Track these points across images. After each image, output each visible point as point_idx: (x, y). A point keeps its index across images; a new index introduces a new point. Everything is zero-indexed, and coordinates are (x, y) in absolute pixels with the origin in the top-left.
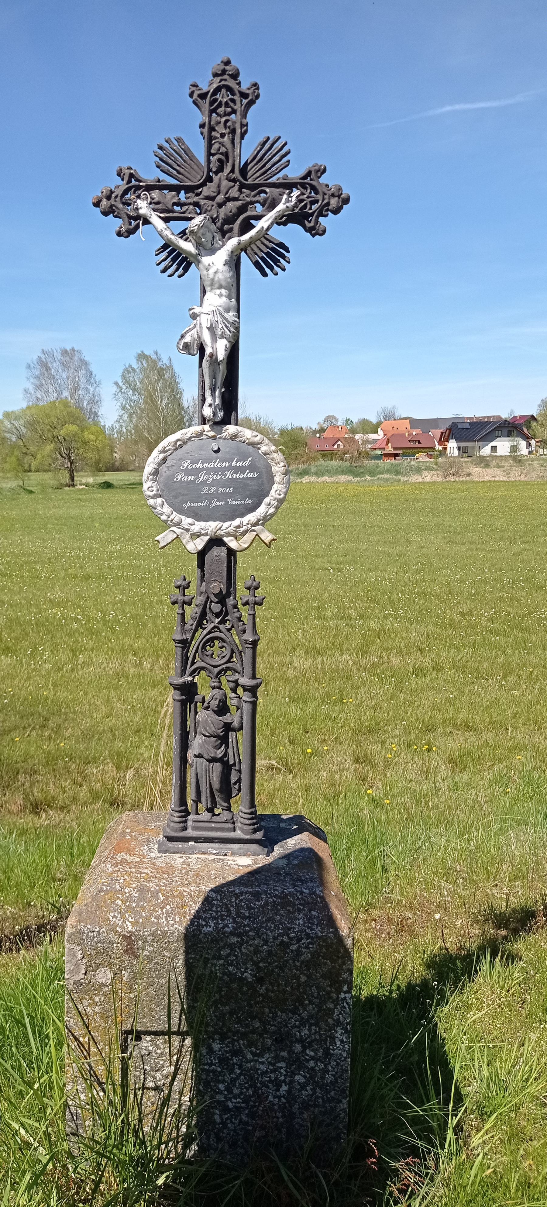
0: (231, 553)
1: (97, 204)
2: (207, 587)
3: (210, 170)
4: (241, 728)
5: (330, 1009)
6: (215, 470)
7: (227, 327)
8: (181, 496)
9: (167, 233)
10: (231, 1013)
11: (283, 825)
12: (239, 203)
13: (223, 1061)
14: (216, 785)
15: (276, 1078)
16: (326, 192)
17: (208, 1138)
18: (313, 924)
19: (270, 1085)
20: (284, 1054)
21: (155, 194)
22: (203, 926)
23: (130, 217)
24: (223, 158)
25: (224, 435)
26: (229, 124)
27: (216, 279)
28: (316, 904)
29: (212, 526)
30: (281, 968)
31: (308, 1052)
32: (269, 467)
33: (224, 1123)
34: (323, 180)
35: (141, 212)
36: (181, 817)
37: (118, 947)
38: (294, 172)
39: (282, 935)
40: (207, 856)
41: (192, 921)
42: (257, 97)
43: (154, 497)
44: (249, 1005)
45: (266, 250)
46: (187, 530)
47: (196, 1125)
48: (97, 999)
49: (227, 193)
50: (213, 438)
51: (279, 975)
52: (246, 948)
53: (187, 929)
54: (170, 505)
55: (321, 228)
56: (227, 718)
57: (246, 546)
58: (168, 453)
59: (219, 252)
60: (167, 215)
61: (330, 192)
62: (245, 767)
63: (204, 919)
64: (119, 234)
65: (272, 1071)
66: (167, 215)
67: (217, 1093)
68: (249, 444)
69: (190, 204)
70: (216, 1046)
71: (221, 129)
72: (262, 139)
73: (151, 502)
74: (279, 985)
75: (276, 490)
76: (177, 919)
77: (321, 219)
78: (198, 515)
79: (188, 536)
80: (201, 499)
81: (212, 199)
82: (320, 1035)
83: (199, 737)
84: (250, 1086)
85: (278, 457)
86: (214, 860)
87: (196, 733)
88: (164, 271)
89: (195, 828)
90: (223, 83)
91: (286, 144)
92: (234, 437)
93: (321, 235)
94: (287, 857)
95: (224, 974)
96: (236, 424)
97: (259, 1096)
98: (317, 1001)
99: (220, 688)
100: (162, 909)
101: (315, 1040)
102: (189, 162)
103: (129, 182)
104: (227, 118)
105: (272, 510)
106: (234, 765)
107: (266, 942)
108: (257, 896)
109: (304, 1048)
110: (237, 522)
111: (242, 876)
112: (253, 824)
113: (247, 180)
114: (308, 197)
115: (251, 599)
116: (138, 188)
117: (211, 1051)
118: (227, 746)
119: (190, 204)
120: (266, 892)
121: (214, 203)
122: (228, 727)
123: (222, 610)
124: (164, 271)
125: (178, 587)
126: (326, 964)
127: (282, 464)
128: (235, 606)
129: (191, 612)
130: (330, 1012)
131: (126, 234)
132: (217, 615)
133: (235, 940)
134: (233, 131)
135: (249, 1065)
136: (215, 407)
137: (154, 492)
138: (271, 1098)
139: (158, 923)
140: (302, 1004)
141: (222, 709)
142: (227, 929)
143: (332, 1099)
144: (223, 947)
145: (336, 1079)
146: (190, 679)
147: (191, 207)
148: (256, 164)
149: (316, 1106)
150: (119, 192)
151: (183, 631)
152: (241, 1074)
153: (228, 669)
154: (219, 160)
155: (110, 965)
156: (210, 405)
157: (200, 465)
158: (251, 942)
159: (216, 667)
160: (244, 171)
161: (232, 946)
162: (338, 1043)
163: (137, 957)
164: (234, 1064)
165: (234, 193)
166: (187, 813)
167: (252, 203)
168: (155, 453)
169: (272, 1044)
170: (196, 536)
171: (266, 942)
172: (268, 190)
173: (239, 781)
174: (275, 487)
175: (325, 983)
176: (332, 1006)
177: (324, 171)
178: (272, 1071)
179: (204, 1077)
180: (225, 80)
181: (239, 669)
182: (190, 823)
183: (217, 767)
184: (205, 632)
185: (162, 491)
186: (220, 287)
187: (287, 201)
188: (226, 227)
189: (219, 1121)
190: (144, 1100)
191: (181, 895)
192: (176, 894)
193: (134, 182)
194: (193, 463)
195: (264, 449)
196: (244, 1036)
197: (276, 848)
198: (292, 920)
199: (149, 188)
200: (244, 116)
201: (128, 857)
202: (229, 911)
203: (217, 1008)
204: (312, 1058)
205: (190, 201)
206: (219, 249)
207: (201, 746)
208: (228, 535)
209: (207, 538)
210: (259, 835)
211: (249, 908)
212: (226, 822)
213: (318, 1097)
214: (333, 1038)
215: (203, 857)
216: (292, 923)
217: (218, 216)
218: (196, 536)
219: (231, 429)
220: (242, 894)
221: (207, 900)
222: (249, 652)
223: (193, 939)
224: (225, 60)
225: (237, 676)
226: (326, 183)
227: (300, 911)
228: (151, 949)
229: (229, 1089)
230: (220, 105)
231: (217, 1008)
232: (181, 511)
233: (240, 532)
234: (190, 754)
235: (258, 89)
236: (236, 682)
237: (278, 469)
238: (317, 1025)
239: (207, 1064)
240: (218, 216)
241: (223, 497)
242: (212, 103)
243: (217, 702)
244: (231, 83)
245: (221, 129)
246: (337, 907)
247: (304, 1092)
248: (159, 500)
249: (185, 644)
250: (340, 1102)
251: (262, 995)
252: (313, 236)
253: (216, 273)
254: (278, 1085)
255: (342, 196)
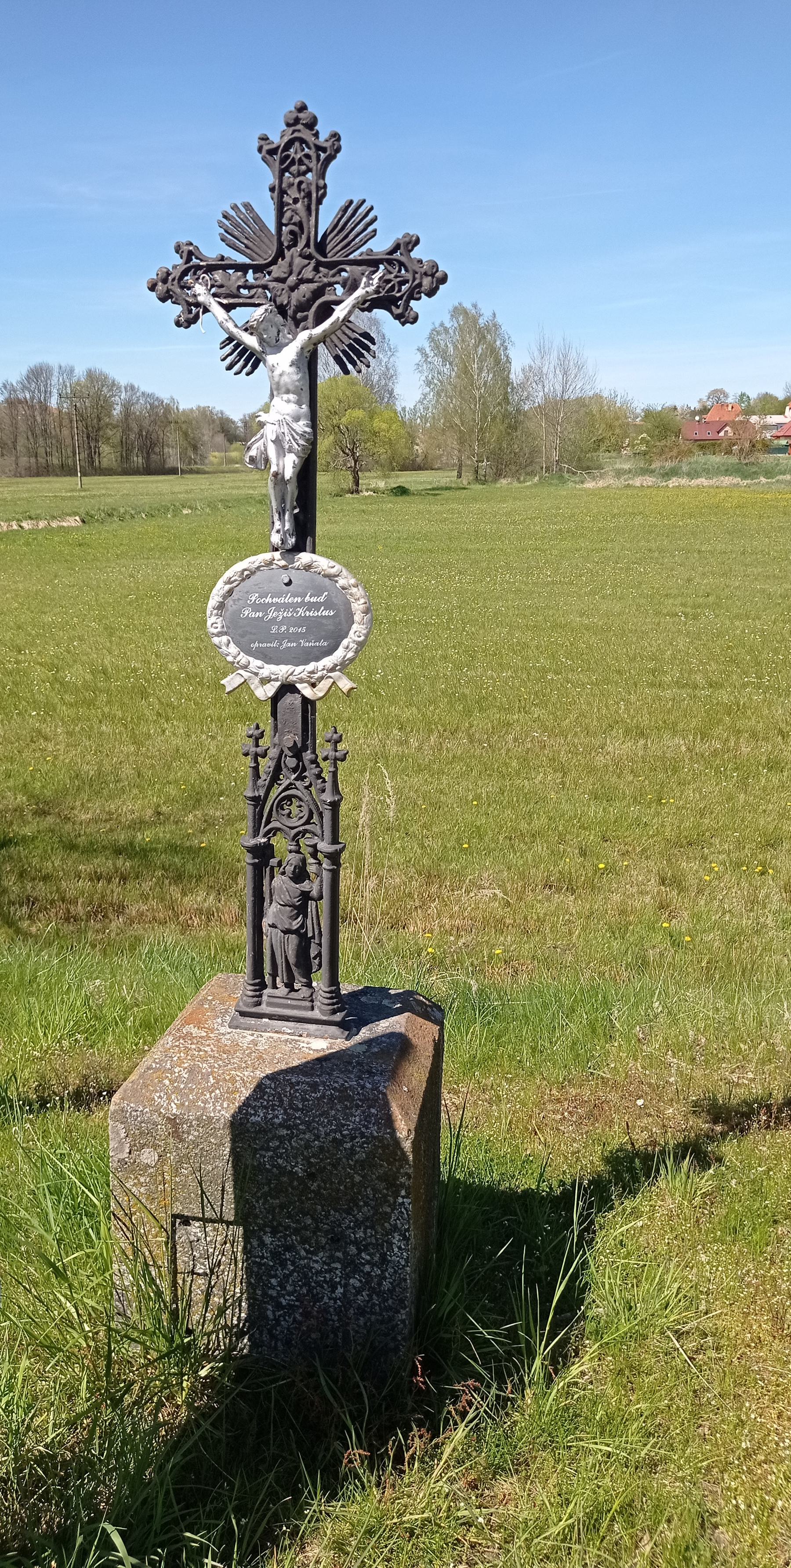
0: (306, 702)
1: (152, 288)
2: (280, 740)
3: (280, 243)
4: (321, 897)
5: (386, 1213)
6: (286, 606)
7: (295, 440)
8: (251, 635)
9: (230, 325)
10: (282, 1207)
11: (386, 1002)
12: (314, 286)
13: (275, 1255)
14: (292, 960)
15: (331, 1279)
16: (418, 270)
17: (261, 1334)
18: (369, 1122)
19: (325, 1286)
20: (339, 1254)
21: (218, 275)
22: (251, 1115)
23: (189, 304)
24: (296, 229)
25: (297, 564)
26: (303, 186)
27: (282, 382)
28: (376, 1101)
29: (282, 671)
30: (334, 1166)
31: (363, 1255)
32: (348, 604)
33: (277, 1321)
34: (416, 254)
35: (201, 299)
36: (255, 991)
37: (162, 1129)
38: (380, 245)
39: (335, 1131)
40: (280, 1036)
41: (240, 1107)
42: (338, 150)
43: (219, 634)
44: (300, 1200)
45: (347, 341)
46: (256, 674)
47: (246, 1320)
48: (142, 1180)
49: (299, 273)
50: (285, 568)
51: (331, 1173)
52: (296, 1142)
53: (233, 1116)
54: (237, 644)
55: (412, 314)
56: (305, 886)
57: (321, 694)
58: (234, 584)
59: (285, 349)
60: (232, 301)
61: (423, 270)
62: (325, 940)
63: (254, 1108)
64: (178, 324)
65: (326, 1271)
66: (232, 301)
67: (270, 1288)
68: (325, 576)
69: (258, 287)
70: (268, 1239)
71: (294, 193)
72: (342, 203)
73: (216, 640)
74: (332, 1183)
75: (357, 631)
76: (225, 1105)
77: (413, 303)
78: (268, 657)
79: (256, 681)
80: (270, 638)
81: (283, 280)
82: (377, 1239)
83: (274, 904)
84: (304, 1285)
85: (358, 592)
86: (287, 1041)
87: (271, 901)
88: (229, 368)
89: (269, 1004)
90: (296, 135)
91: (372, 208)
92: (308, 567)
93: (412, 323)
94: (369, 1042)
95: (273, 1166)
96: (314, 552)
97: (313, 1296)
98: (373, 1203)
99: (298, 852)
100: (211, 1093)
101: (371, 1243)
102: (259, 233)
103: (189, 260)
104: (301, 178)
105: (350, 655)
106: (313, 937)
107: (317, 1137)
108: (314, 1087)
109: (360, 1251)
110: (311, 666)
111: (308, 1062)
112: (333, 1004)
113: (326, 257)
114: (396, 277)
115: (332, 754)
116: (198, 267)
117: (262, 1244)
118: (305, 916)
119: (258, 287)
120: (324, 1084)
121: (285, 286)
122: (306, 896)
123: (298, 765)
124: (229, 368)
125: (250, 736)
126: (382, 1166)
127: (362, 601)
128: (314, 761)
129: (266, 765)
130: (386, 1217)
131: (185, 324)
132: (294, 770)
133: (285, 1132)
134: (309, 195)
135: (302, 1262)
136: (285, 533)
137: (219, 630)
138: (326, 1299)
139: (205, 1108)
140: (357, 1205)
141: (300, 875)
142: (276, 1120)
143: (390, 1308)
144: (272, 1139)
145: (394, 1288)
146: (264, 840)
147: (260, 290)
148: (337, 235)
149: (372, 1313)
150: (176, 274)
151: (255, 787)
152: (293, 1271)
153: (306, 831)
154: (292, 232)
155: (155, 1147)
156: (278, 531)
157: (268, 600)
158: (301, 1136)
159: (292, 828)
160: (321, 247)
161: (281, 1139)
162: (396, 1250)
163: (182, 1140)
164: (286, 1259)
165: (308, 273)
166: (263, 986)
167: (331, 284)
168: (220, 583)
169: (327, 1243)
170: (265, 681)
171: (317, 1137)
172: (348, 268)
173: (319, 955)
174: (355, 627)
175: (382, 1186)
176: (389, 1210)
177: (417, 242)
178: (326, 1271)
179: (255, 1269)
180: (299, 131)
181: (319, 832)
182: (265, 998)
183: (293, 939)
184: (283, 787)
185: (228, 627)
186: (288, 392)
187: (368, 285)
188: (299, 315)
189: (271, 1317)
190: (194, 1287)
191: (233, 1080)
192: (228, 1078)
193: (195, 261)
194: (261, 597)
195: (342, 582)
196: (296, 1232)
197: (363, 1030)
198: (347, 1117)
199: (210, 269)
200: (322, 175)
201: (195, 1031)
202: (281, 1101)
203: (266, 1201)
204: (368, 1262)
205: (259, 282)
206: (287, 344)
207: (276, 916)
208: (302, 681)
209: (278, 684)
210: (338, 1017)
211: (304, 1100)
212: (304, 999)
213: (374, 1304)
214: (391, 1244)
215: (276, 1036)
216: (347, 1119)
217: (289, 302)
218: (265, 681)
219: (305, 557)
220: (298, 1083)
221: (260, 1087)
222: (327, 816)
223: (239, 1126)
224: (299, 105)
225: (316, 840)
226: (418, 257)
227: (358, 1106)
228: (196, 1133)
229: (282, 1285)
230: (293, 163)
231: (266, 1201)
232: (249, 652)
233: (320, 677)
234: (266, 922)
235: (339, 139)
236: (314, 846)
237: (358, 607)
238: (372, 1227)
239: (258, 1257)
240: (289, 302)
241: (296, 637)
242: (282, 161)
243: (292, 868)
244: (306, 135)
245: (294, 193)
246: (402, 1107)
247: (359, 1297)
248: (224, 639)
249: (258, 802)
250: (399, 1312)
251: (313, 1191)
252: (403, 324)
253: (281, 375)
254: (333, 1287)
255: (437, 275)
